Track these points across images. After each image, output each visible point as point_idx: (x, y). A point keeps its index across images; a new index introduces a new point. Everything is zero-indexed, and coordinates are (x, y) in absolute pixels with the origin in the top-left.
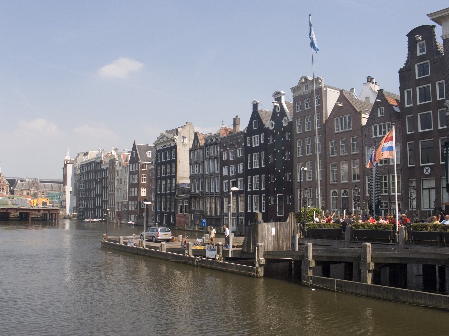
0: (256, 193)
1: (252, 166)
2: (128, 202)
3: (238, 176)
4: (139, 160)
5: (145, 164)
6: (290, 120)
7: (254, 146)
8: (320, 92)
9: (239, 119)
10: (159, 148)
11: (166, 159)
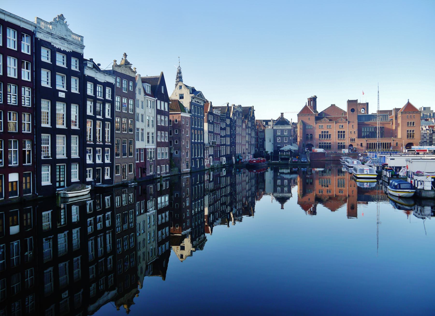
2: (156, 149)
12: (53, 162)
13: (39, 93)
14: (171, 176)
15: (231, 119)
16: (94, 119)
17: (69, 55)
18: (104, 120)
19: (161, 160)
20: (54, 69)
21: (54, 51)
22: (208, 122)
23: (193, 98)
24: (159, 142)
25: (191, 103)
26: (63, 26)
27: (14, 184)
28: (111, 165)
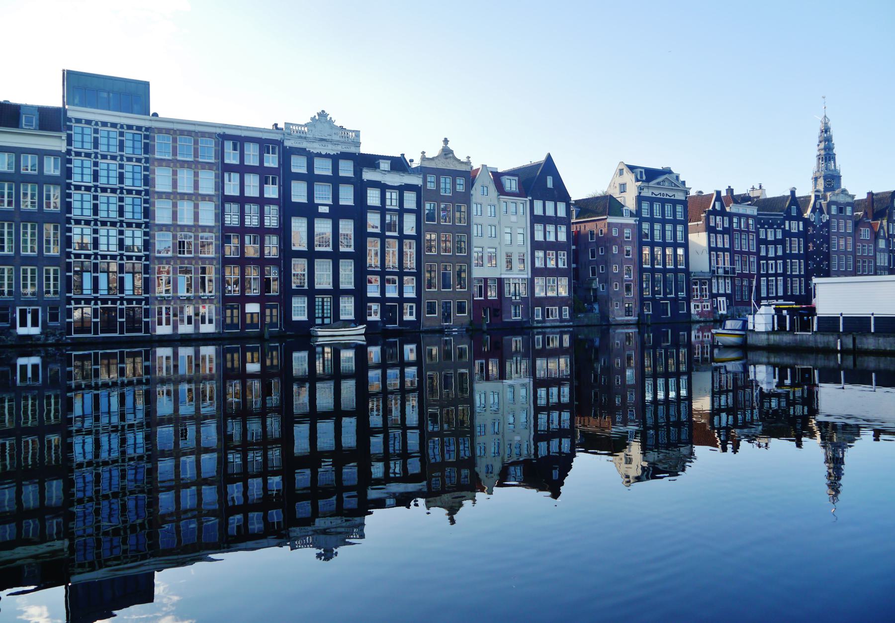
0: (796, 276)
1: (791, 250)
3: (776, 258)
12: (311, 293)
13: (288, 209)
14: (578, 326)
15: (807, 222)
16: (382, 237)
17: (335, 159)
18: (402, 238)
20: (311, 179)
21: (311, 157)
22: (711, 230)
23: (641, 189)
25: (640, 199)
26: (326, 125)
27: (255, 316)
28: (417, 300)
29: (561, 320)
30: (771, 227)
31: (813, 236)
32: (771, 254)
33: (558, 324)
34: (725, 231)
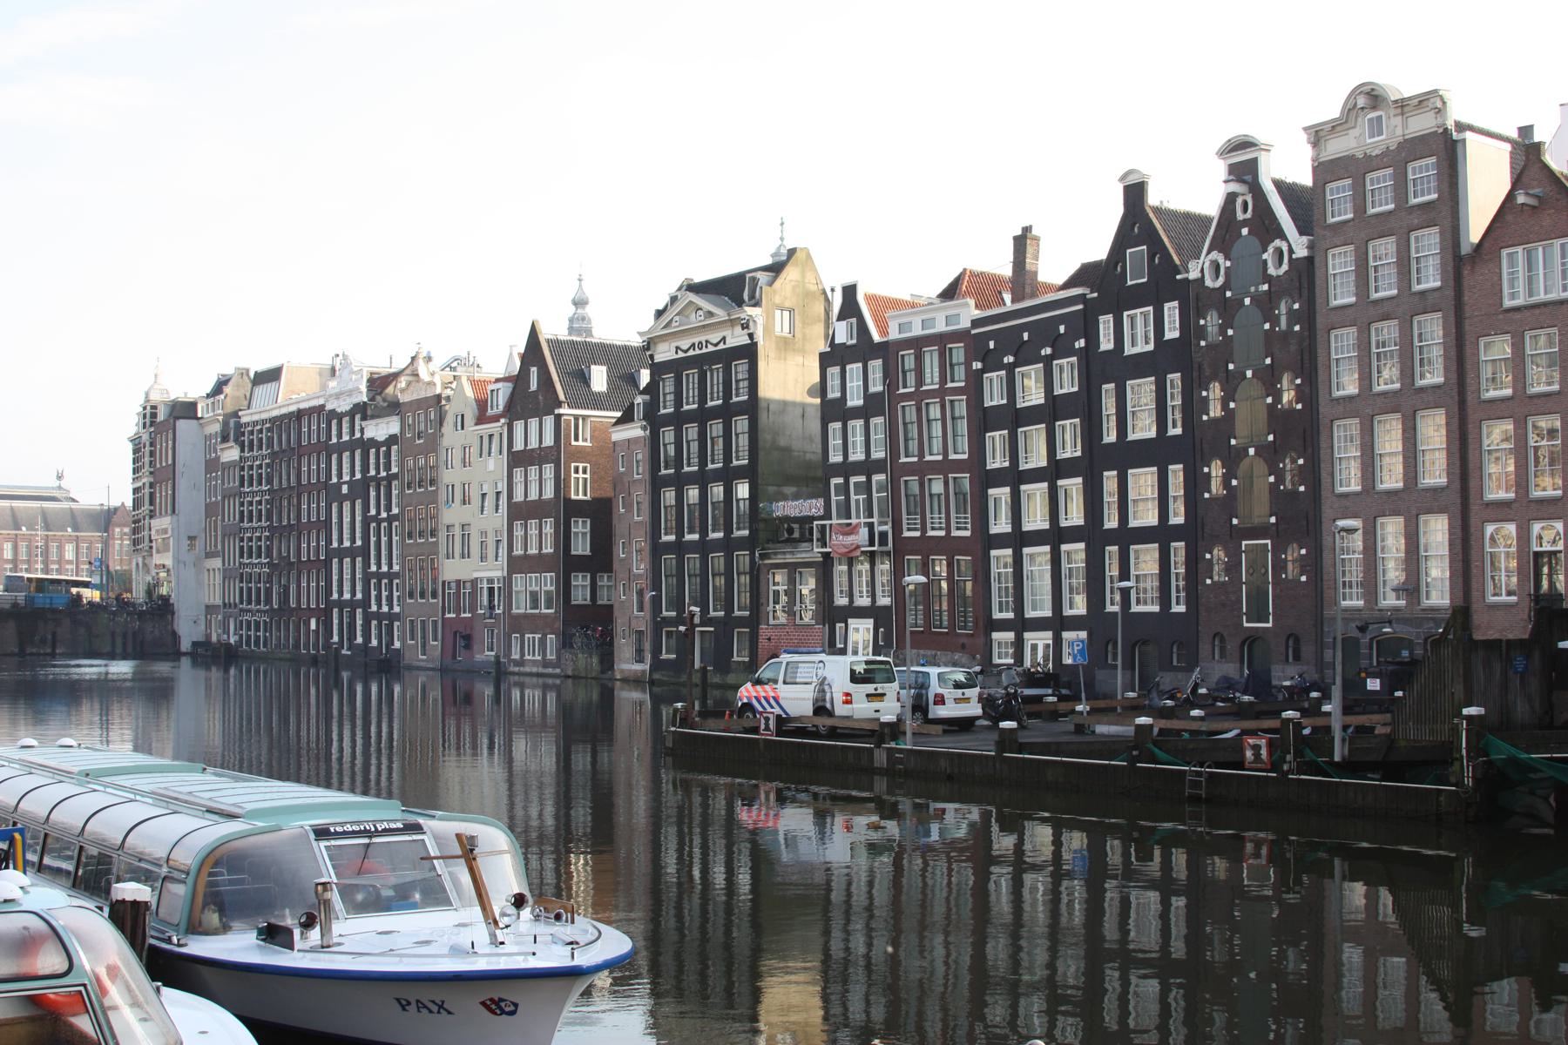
0: (1144, 535)
2: (508, 581)
3: (1055, 470)
4: (559, 405)
5: (584, 418)
6: (1300, 252)
7: (1129, 350)
8: (1447, 149)
9: (1037, 239)
10: (664, 353)
11: (703, 399)
19: (525, 616)
24: (519, 557)
29: (546, 663)
30: (1026, 355)
31: (1224, 350)
32: (1036, 456)
33: (541, 670)
34: (872, 407)
